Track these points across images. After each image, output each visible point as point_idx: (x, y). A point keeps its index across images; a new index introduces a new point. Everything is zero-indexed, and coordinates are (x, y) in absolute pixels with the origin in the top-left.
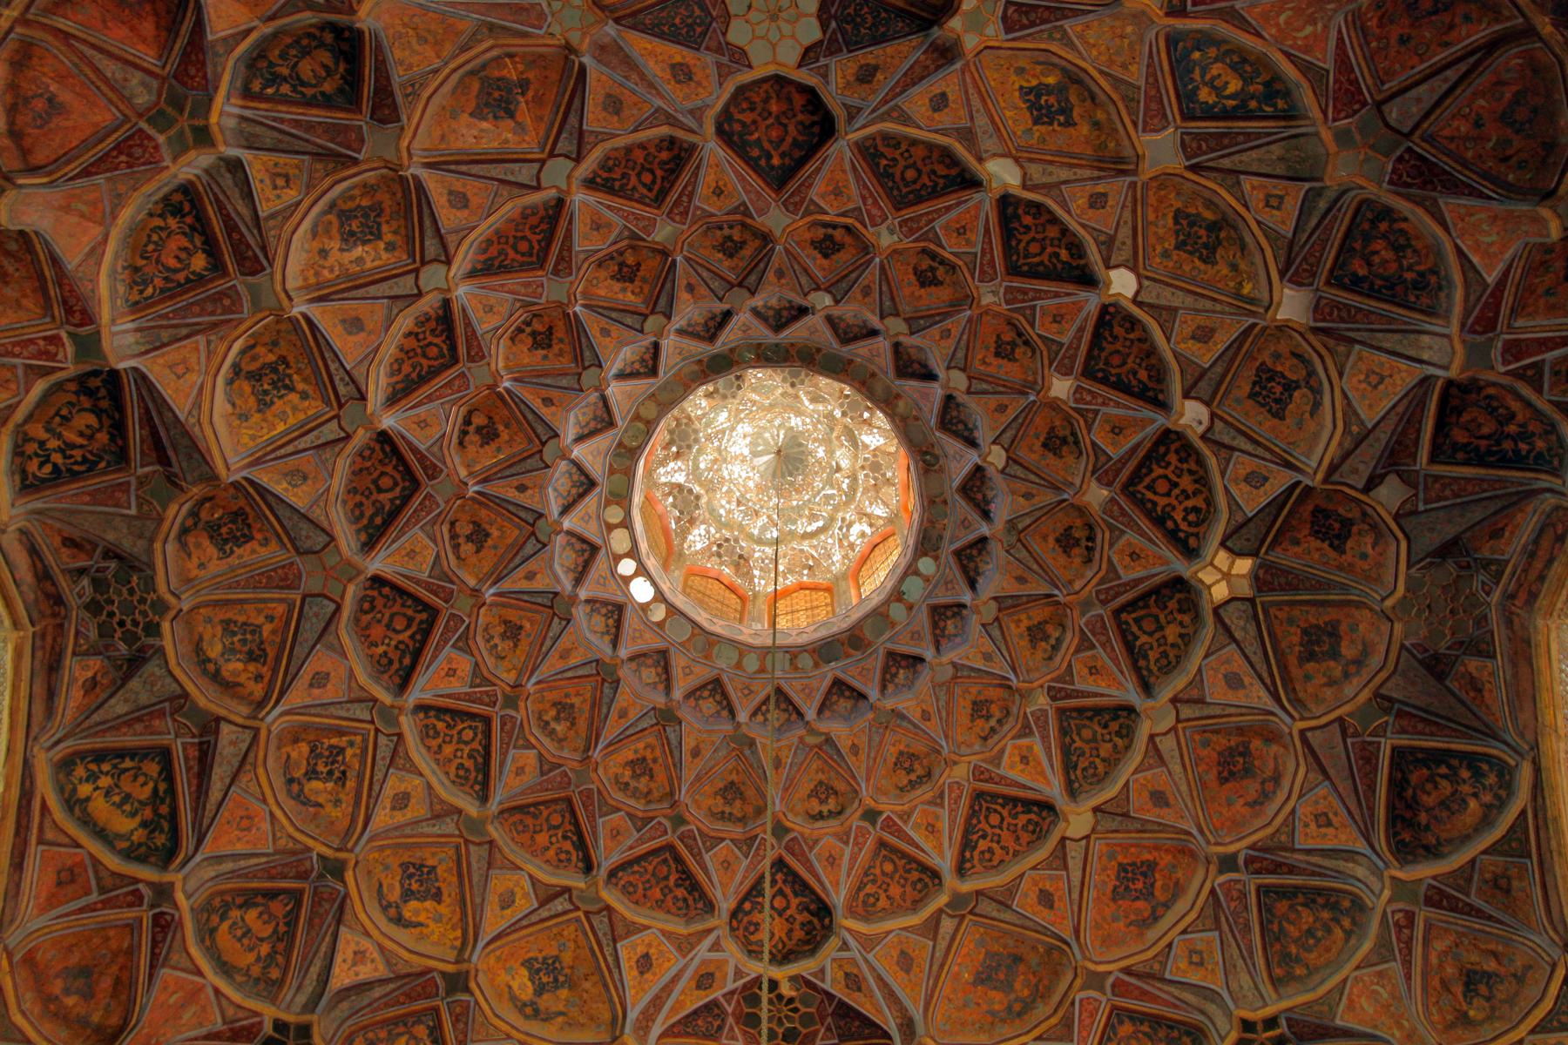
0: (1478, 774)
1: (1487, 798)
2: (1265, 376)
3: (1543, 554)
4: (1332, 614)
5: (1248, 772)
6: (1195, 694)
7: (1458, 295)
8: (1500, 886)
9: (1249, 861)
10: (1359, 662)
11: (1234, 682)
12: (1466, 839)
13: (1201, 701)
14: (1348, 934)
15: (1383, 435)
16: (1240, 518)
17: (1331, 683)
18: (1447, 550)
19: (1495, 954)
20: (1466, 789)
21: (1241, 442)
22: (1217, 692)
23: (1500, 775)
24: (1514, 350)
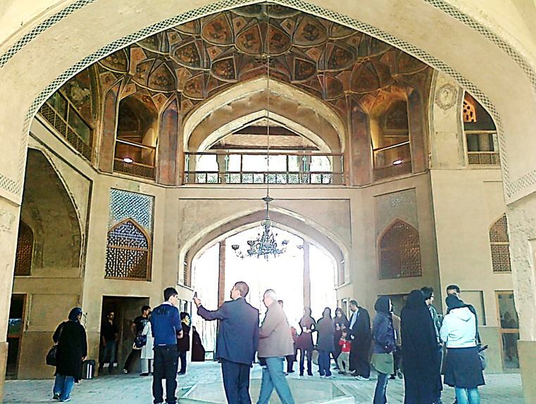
0: (230, 71)
1: (226, 74)
2: (314, 27)
3: (279, 75)
4: (257, 38)
5: (216, 30)
6: (233, 16)
7: (333, 71)
8: (212, 83)
9: (200, 41)
10: (248, 47)
11: (238, 24)
12: (218, 75)
13: (232, 19)
14: (191, 62)
15: (303, 54)
16: (279, 22)
17: (243, 43)
18: (277, 61)
19: (198, 86)
20: (226, 69)
21: (297, 24)
22: (235, 21)
23: (231, 75)
24: (321, 77)
